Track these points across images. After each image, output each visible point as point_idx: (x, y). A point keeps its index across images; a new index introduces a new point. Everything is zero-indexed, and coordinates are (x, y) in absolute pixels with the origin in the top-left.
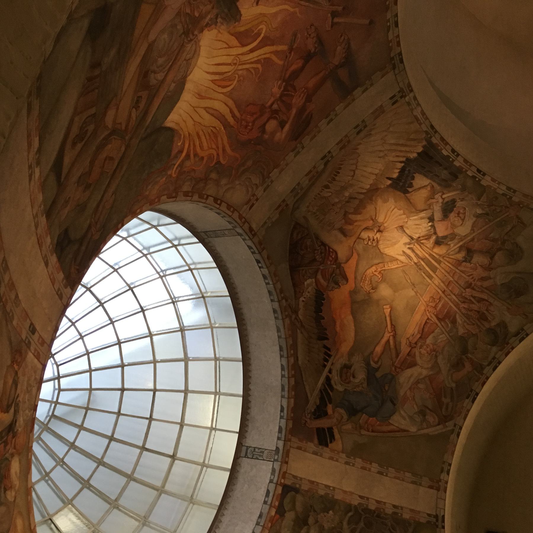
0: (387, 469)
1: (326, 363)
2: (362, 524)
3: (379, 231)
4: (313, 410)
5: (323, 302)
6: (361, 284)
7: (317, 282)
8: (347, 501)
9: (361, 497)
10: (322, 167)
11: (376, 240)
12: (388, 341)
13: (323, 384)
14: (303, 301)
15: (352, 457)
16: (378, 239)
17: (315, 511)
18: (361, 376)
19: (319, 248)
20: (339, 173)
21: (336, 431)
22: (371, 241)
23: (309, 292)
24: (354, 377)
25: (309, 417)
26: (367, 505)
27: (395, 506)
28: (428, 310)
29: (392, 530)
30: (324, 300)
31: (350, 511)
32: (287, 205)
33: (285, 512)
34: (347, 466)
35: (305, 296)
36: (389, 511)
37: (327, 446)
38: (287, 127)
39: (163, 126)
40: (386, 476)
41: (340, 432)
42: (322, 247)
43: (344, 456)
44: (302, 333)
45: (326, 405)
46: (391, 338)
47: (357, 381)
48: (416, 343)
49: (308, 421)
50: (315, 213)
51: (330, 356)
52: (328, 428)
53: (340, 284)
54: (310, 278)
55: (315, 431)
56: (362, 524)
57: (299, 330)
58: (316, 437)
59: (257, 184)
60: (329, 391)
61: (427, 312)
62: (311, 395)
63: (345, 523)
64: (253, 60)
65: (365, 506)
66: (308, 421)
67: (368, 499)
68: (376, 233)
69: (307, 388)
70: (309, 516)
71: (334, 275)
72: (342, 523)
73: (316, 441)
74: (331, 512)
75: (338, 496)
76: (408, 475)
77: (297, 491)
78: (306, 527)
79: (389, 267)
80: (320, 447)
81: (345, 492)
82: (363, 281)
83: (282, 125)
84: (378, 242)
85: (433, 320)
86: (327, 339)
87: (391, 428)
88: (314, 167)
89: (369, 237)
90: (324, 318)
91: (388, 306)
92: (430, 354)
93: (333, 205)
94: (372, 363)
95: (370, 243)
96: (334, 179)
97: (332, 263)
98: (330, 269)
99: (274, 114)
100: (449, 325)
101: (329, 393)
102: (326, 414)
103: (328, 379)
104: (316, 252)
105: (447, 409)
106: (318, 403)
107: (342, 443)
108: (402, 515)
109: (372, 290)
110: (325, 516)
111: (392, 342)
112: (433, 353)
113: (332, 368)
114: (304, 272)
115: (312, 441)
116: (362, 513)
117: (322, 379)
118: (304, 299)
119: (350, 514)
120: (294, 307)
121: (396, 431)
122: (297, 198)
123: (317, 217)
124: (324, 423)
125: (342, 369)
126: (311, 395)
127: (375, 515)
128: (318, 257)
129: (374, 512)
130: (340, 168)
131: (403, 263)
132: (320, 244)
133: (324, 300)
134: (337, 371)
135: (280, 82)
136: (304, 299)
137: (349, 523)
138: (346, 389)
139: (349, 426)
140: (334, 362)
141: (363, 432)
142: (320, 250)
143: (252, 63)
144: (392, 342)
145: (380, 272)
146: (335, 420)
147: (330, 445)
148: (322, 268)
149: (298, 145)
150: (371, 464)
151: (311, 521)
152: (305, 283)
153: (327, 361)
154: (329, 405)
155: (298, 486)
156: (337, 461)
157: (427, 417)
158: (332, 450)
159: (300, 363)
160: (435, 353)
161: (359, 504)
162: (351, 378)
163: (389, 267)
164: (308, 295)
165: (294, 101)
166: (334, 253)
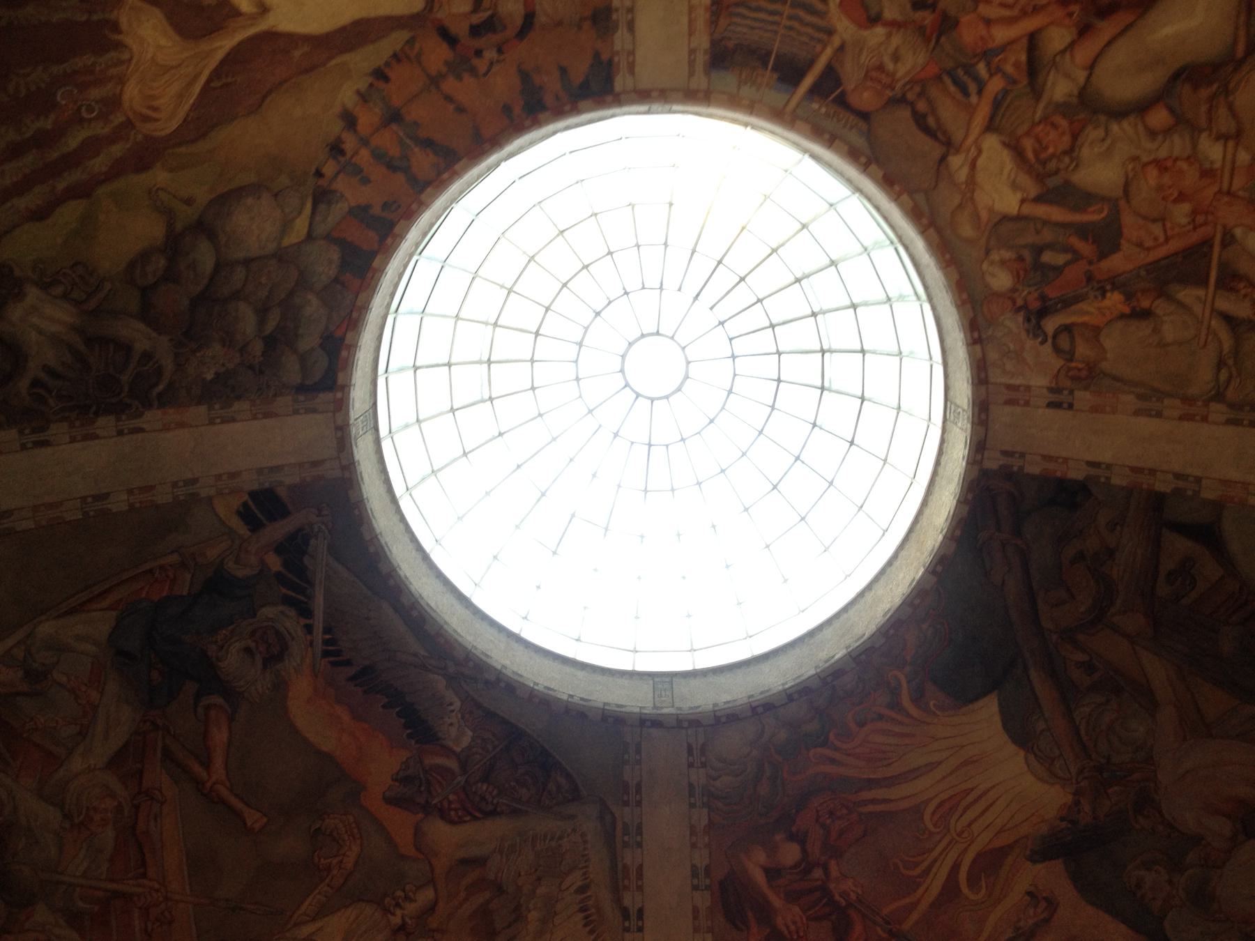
1: (327, 637)
2: (125, 378)
3: (402, 927)
4: (312, 542)
5: (409, 731)
6: (352, 819)
7: (448, 752)
8: (171, 411)
10: (627, 901)
11: (392, 908)
12: (207, 765)
14: (451, 704)
15: (182, 498)
16: (389, 916)
17: (251, 367)
18: (232, 661)
19: (495, 801)
20: (585, 926)
22: (400, 901)
23: (451, 724)
24: (248, 650)
25: (316, 526)
27: (45, 443)
28: (157, 891)
29: (42, 392)
30: (410, 736)
31: (160, 395)
32: (626, 804)
33: (321, 346)
35: (454, 714)
36: (58, 430)
37: (253, 495)
38: (759, 877)
39: (996, 692)
40: (84, 499)
42: (490, 808)
44: (415, 655)
46: (204, 775)
48: (137, 807)
50: (561, 838)
51: (326, 654)
52: (263, 525)
53: (397, 784)
54: (469, 747)
56: (125, 378)
57: (423, 656)
59: (715, 779)
60: (290, 593)
61: (157, 886)
63: (169, 365)
64: (938, 864)
65: (124, 417)
67: (120, 433)
68: (403, 920)
70: (262, 355)
71: (423, 788)
73: (282, 492)
74: (209, 376)
77: (301, 389)
78: (267, 333)
79: (319, 893)
80: (267, 485)
81: (182, 425)
82: (353, 825)
83: (772, 873)
84: (386, 911)
85: (131, 882)
86: (352, 679)
88: (640, 888)
89: (412, 900)
90: (384, 706)
91: (257, 826)
92: (88, 808)
93: (539, 879)
94: (219, 700)
95: (399, 893)
96: (583, 909)
97: (445, 804)
98: (440, 791)
99: (804, 866)
100: (81, 904)
102: (279, 549)
104: (495, 792)
106: (306, 560)
107: (217, 515)
108: (21, 432)
109: (318, 826)
110: (223, 365)
111: (197, 769)
112: (82, 817)
113: (309, 637)
114: (490, 748)
117: (319, 604)
118: (452, 708)
119: (161, 387)
121: (90, 601)
122: (619, 826)
123: (549, 837)
124: (277, 531)
127: (94, 408)
128: (485, 788)
129: (97, 414)
130: (591, 932)
131: (297, 925)
132: (499, 809)
133: (410, 736)
134: (293, 639)
135: (853, 896)
136: (452, 708)
138: (254, 616)
140: (309, 649)
141: (175, 558)
142: (490, 800)
143: (936, 860)
144: (197, 769)
145: (329, 868)
147: (246, 497)
148: (459, 778)
149: (708, 881)
151: (258, 347)
152: (470, 733)
153: (326, 642)
154: (281, 569)
155: (302, 398)
156: (219, 477)
157: (21, 673)
160: (76, 821)
161: (141, 415)
162: (252, 645)
163: (319, 893)
164: (449, 721)
165: (797, 909)
166: (456, 819)
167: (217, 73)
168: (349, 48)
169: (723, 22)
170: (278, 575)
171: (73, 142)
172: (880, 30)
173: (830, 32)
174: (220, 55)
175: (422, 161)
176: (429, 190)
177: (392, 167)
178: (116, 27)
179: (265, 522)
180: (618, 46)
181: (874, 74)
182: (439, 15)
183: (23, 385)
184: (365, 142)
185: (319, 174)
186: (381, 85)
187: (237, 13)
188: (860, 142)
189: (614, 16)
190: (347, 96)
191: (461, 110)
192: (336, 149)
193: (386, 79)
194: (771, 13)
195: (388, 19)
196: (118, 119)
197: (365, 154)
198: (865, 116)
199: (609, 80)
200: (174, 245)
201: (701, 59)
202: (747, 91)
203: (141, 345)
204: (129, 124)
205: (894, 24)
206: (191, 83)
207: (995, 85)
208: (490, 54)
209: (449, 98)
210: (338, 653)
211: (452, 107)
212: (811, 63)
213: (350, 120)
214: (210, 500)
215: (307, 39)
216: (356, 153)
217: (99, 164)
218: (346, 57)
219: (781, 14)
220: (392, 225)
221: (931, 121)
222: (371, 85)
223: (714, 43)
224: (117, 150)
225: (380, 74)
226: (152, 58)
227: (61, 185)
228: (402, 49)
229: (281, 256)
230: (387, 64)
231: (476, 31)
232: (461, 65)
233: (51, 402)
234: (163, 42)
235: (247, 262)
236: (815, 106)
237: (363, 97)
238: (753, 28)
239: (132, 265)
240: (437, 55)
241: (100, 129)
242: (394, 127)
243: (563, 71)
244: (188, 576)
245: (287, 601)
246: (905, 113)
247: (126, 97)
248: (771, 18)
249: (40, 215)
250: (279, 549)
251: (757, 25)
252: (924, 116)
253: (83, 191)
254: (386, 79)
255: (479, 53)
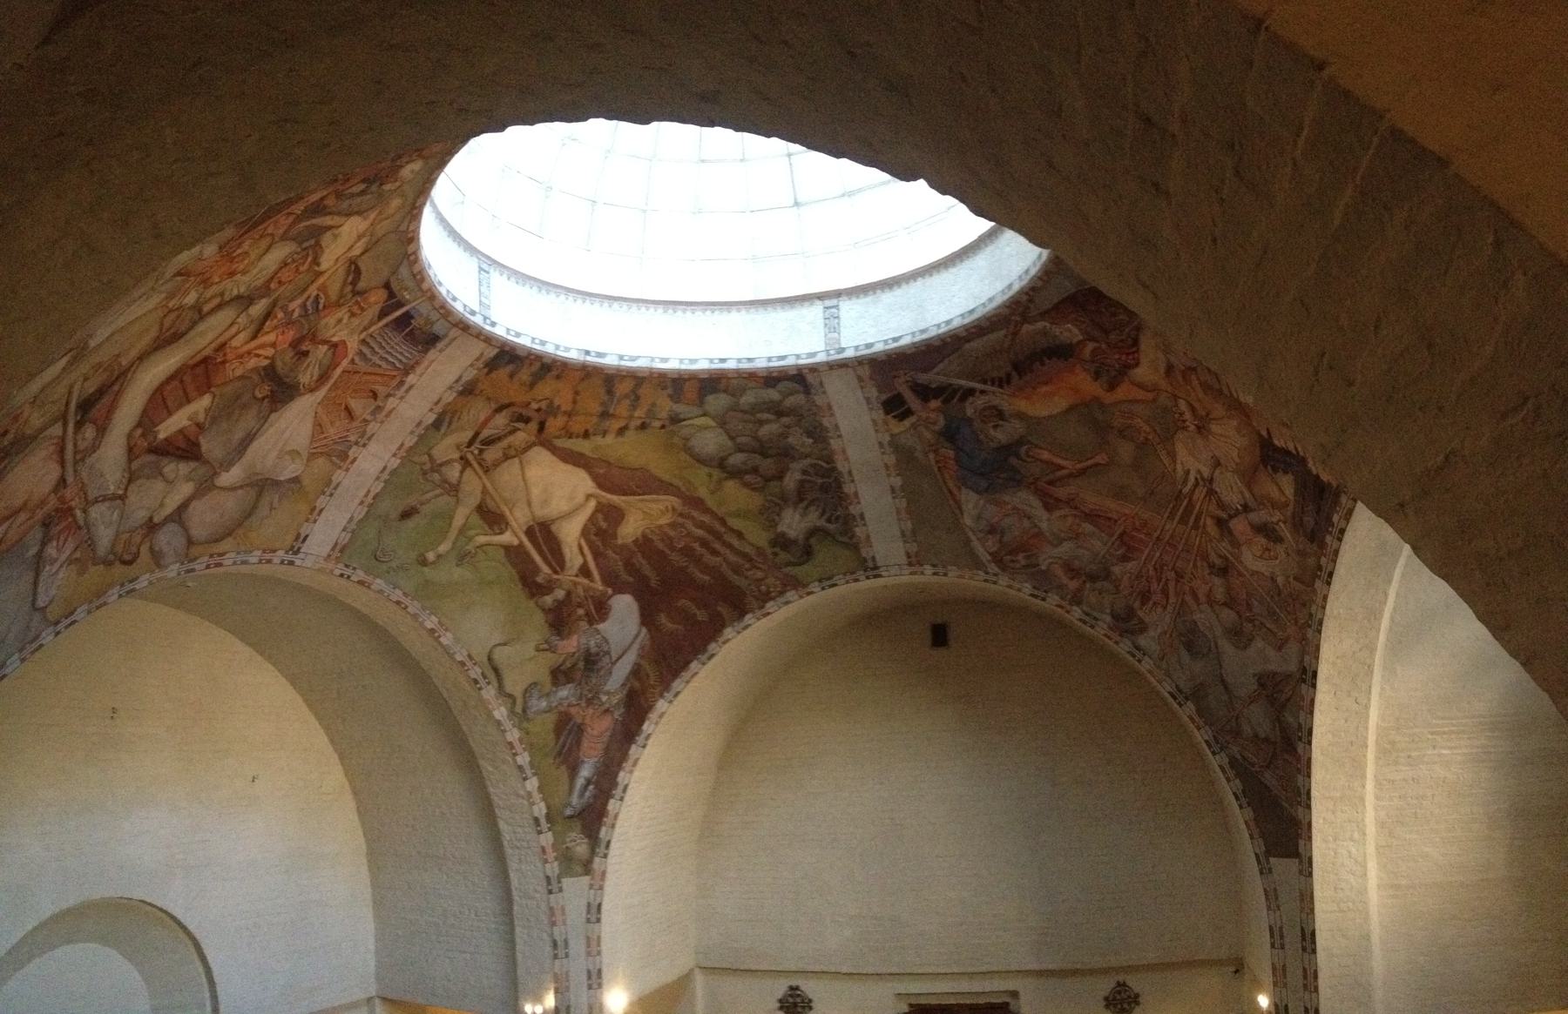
0: (903, 497)
9: (850, 472)
13: (961, 387)
21: (913, 419)
24: (995, 427)
26: (845, 483)
29: (833, 518)
31: (828, 463)
34: (877, 446)
36: (854, 510)
37: (887, 413)
40: (894, 498)
41: (914, 426)
43: (887, 438)
44: (1006, 336)
45: (936, 397)
47: (992, 432)
49: (902, 379)
51: (1001, 386)
55: (895, 392)
56: (820, 481)
58: (889, 395)
60: (957, 397)
62: (938, 374)
63: (808, 461)
66: (902, 379)
69: (941, 366)
72: (806, 457)
73: (884, 397)
74: (811, 441)
75: (835, 444)
76: (909, 524)
87: (955, 491)
101: (953, 398)
102: (926, 400)
103: (971, 392)
105: (1013, 561)
106: (934, 386)
108: (857, 526)
115: (880, 391)
116: (833, 479)
120: (1030, 315)
124: (913, 402)
125: (995, 407)
126: (938, 374)
134: (990, 401)
137: (811, 465)
139: (928, 435)
141: (931, 456)
146: (924, 415)
147: (889, 417)
150: (898, 475)
151: (785, 420)
153: (993, 384)
154: (939, 400)
158: (886, 423)
159: (967, 346)
167: (634, 494)
168: (582, 455)
169: (412, 363)
170: (946, 402)
171: (700, 532)
172: (335, 339)
173: (364, 342)
174: (623, 498)
175: (622, 388)
176: (640, 375)
177: (638, 398)
178: (636, 542)
179: (906, 407)
180: (475, 372)
181: (359, 312)
182: (533, 438)
183: (831, 527)
184: (631, 417)
185: (663, 427)
186: (591, 431)
187: (599, 503)
188: (404, 271)
189: (461, 389)
190: (610, 439)
191: (577, 393)
192: (643, 426)
193: (586, 431)
194: (386, 360)
195: (553, 453)
196: (680, 520)
197: (636, 414)
198: (387, 286)
199: (497, 357)
200: (735, 474)
201: (440, 345)
202: (434, 316)
203: (798, 476)
204: (681, 515)
205: (325, 342)
206: (642, 500)
207: (295, 305)
208: (535, 406)
209: (575, 402)
210: (1001, 380)
211: (578, 398)
212: (386, 325)
213: (621, 431)
214: (892, 435)
215: (591, 473)
216: (641, 418)
217: (706, 519)
218: (588, 453)
219: (381, 357)
220: (674, 380)
221: (350, 278)
222: (595, 435)
223: (426, 351)
224: (695, 514)
225: (586, 435)
226: (642, 520)
227: (723, 530)
228: (564, 437)
229: (722, 423)
230: (577, 437)
231: (527, 420)
232: (552, 410)
233: (839, 513)
234: (632, 519)
235: (732, 438)
236: (408, 297)
237: (604, 433)
238: (401, 353)
239: (754, 489)
240: (554, 424)
241: (690, 525)
242: (611, 411)
243: (511, 376)
244: (943, 450)
245: (963, 399)
246: (361, 285)
247: (668, 521)
248: (387, 356)
249: (740, 535)
250: (926, 400)
251: (398, 355)
252: (351, 283)
253: (723, 522)
254: (586, 431)
255: (539, 410)
